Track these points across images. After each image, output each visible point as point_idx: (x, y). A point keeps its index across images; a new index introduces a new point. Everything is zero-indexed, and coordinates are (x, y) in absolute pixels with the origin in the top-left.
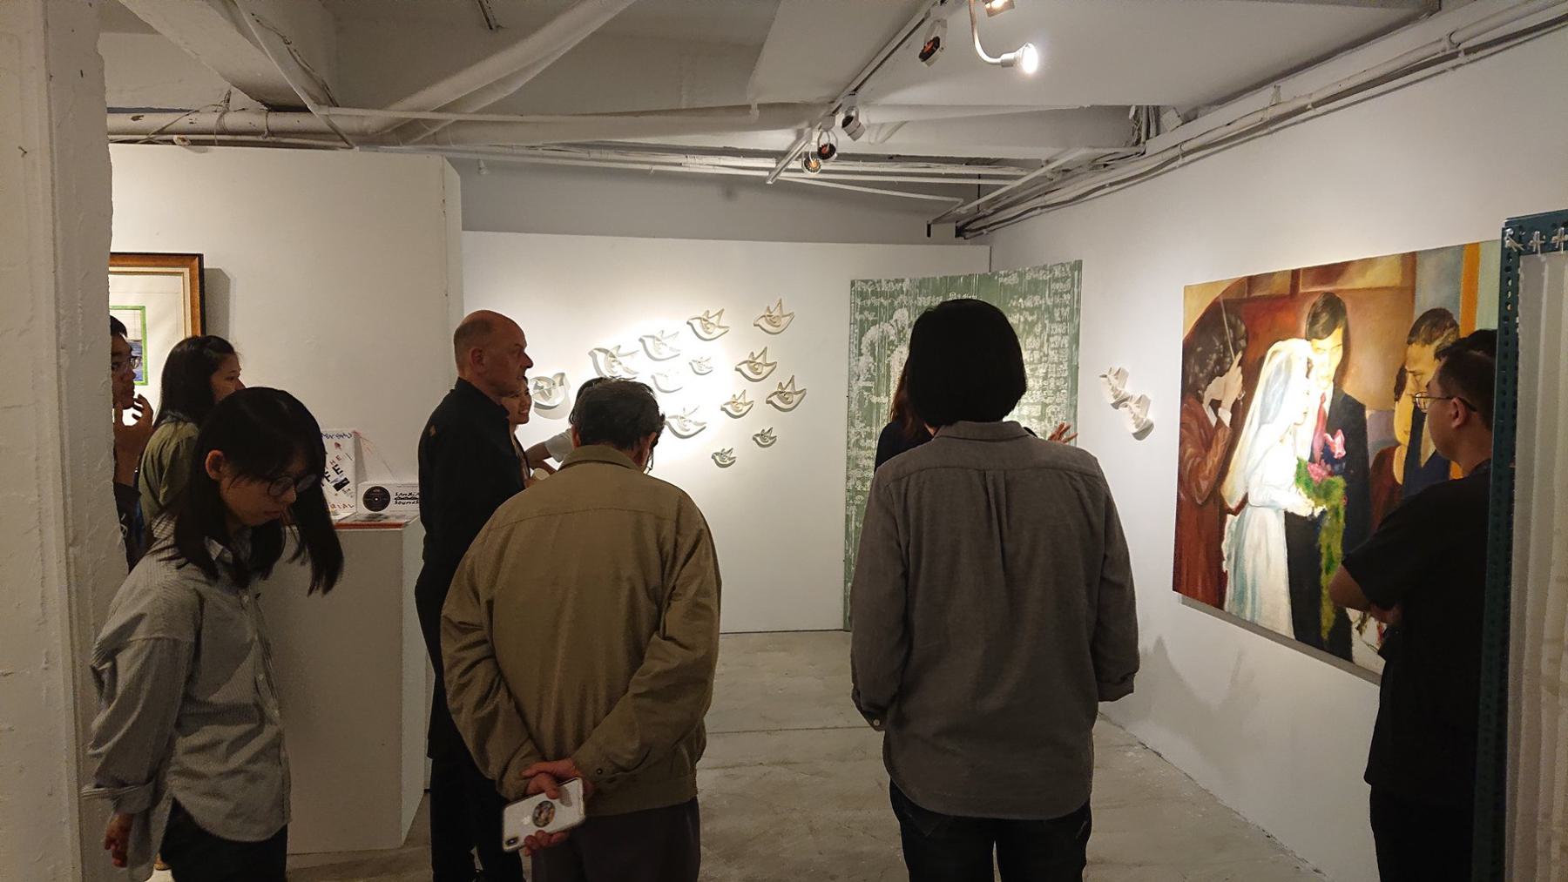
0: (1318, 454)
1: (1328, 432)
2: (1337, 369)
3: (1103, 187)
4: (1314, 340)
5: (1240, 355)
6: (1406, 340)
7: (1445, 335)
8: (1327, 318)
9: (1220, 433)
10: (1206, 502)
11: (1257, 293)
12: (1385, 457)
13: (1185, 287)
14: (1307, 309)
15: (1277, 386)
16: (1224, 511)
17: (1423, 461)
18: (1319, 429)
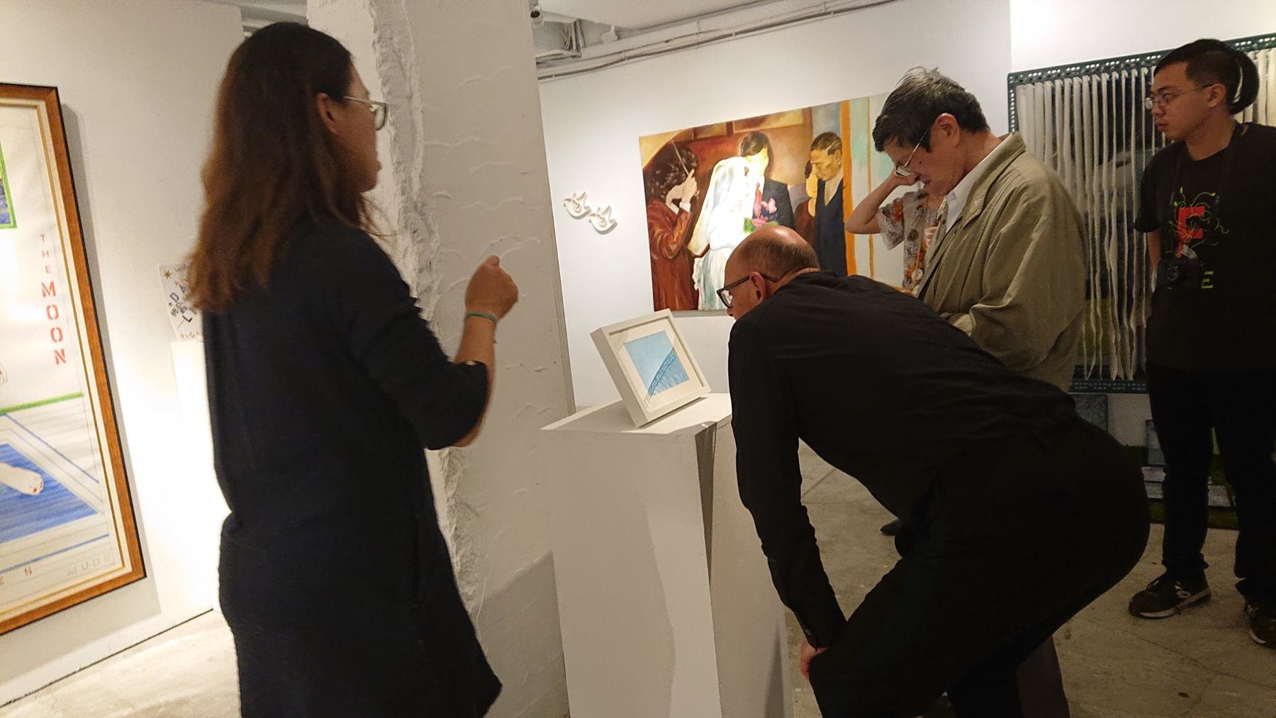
0: (758, 213)
1: (763, 200)
2: (766, 171)
3: (551, 76)
4: (748, 157)
5: (693, 171)
6: (809, 149)
7: (833, 143)
8: (755, 144)
9: (683, 216)
10: (673, 259)
11: (702, 136)
12: (803, 206)
13: (640, 138)
14: (741, 141)
15: (725, 185)
16: (692, 258)
17: (826, 204)
18: (758, 199)
